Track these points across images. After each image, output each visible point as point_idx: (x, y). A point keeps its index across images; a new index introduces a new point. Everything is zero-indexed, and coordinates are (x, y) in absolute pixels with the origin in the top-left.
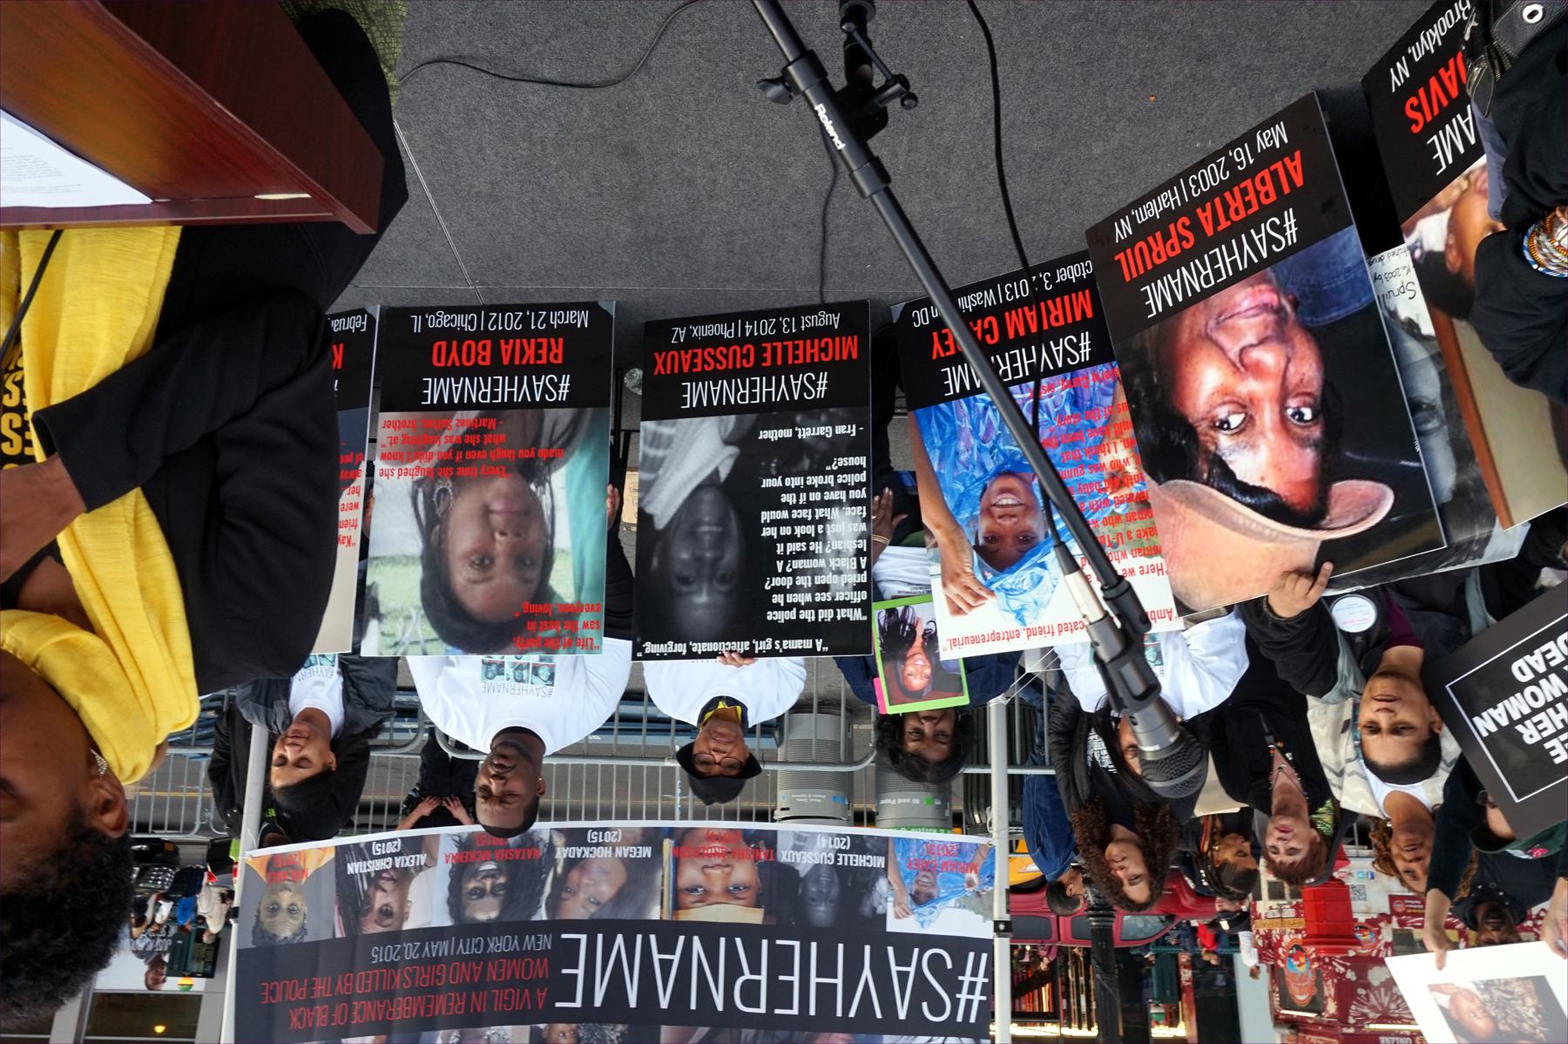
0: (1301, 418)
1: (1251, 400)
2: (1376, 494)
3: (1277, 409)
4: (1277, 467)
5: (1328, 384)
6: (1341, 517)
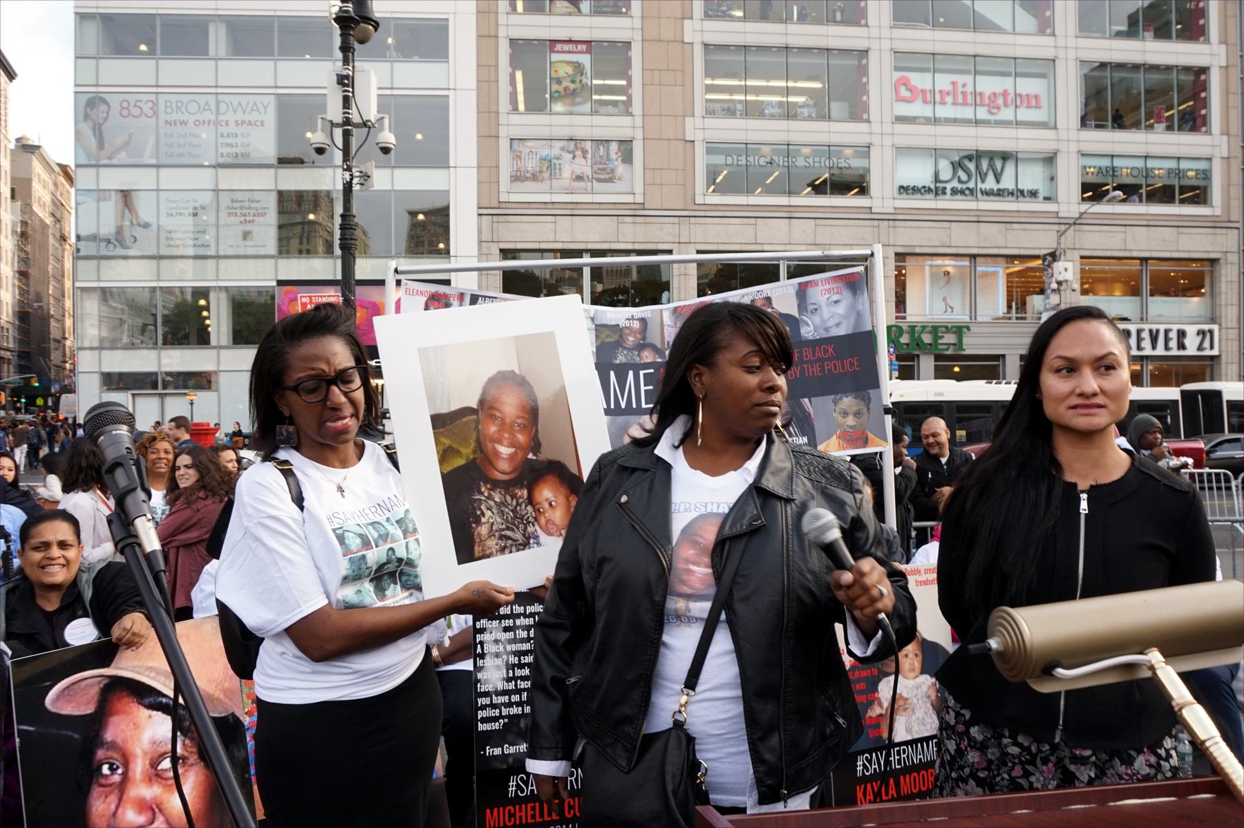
0: (111, 765)
1: (150, 780)
2: (59, 704)
3: (130, 774)
4: (136, 726)
5: (83, 795)
6: (91, 686)
